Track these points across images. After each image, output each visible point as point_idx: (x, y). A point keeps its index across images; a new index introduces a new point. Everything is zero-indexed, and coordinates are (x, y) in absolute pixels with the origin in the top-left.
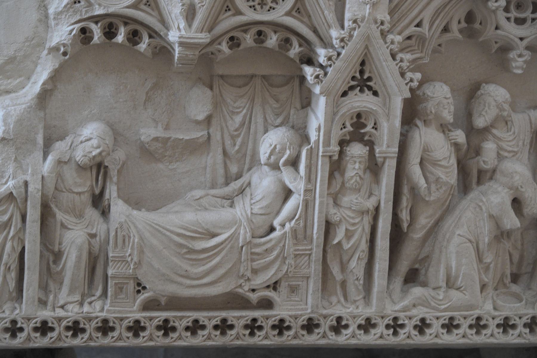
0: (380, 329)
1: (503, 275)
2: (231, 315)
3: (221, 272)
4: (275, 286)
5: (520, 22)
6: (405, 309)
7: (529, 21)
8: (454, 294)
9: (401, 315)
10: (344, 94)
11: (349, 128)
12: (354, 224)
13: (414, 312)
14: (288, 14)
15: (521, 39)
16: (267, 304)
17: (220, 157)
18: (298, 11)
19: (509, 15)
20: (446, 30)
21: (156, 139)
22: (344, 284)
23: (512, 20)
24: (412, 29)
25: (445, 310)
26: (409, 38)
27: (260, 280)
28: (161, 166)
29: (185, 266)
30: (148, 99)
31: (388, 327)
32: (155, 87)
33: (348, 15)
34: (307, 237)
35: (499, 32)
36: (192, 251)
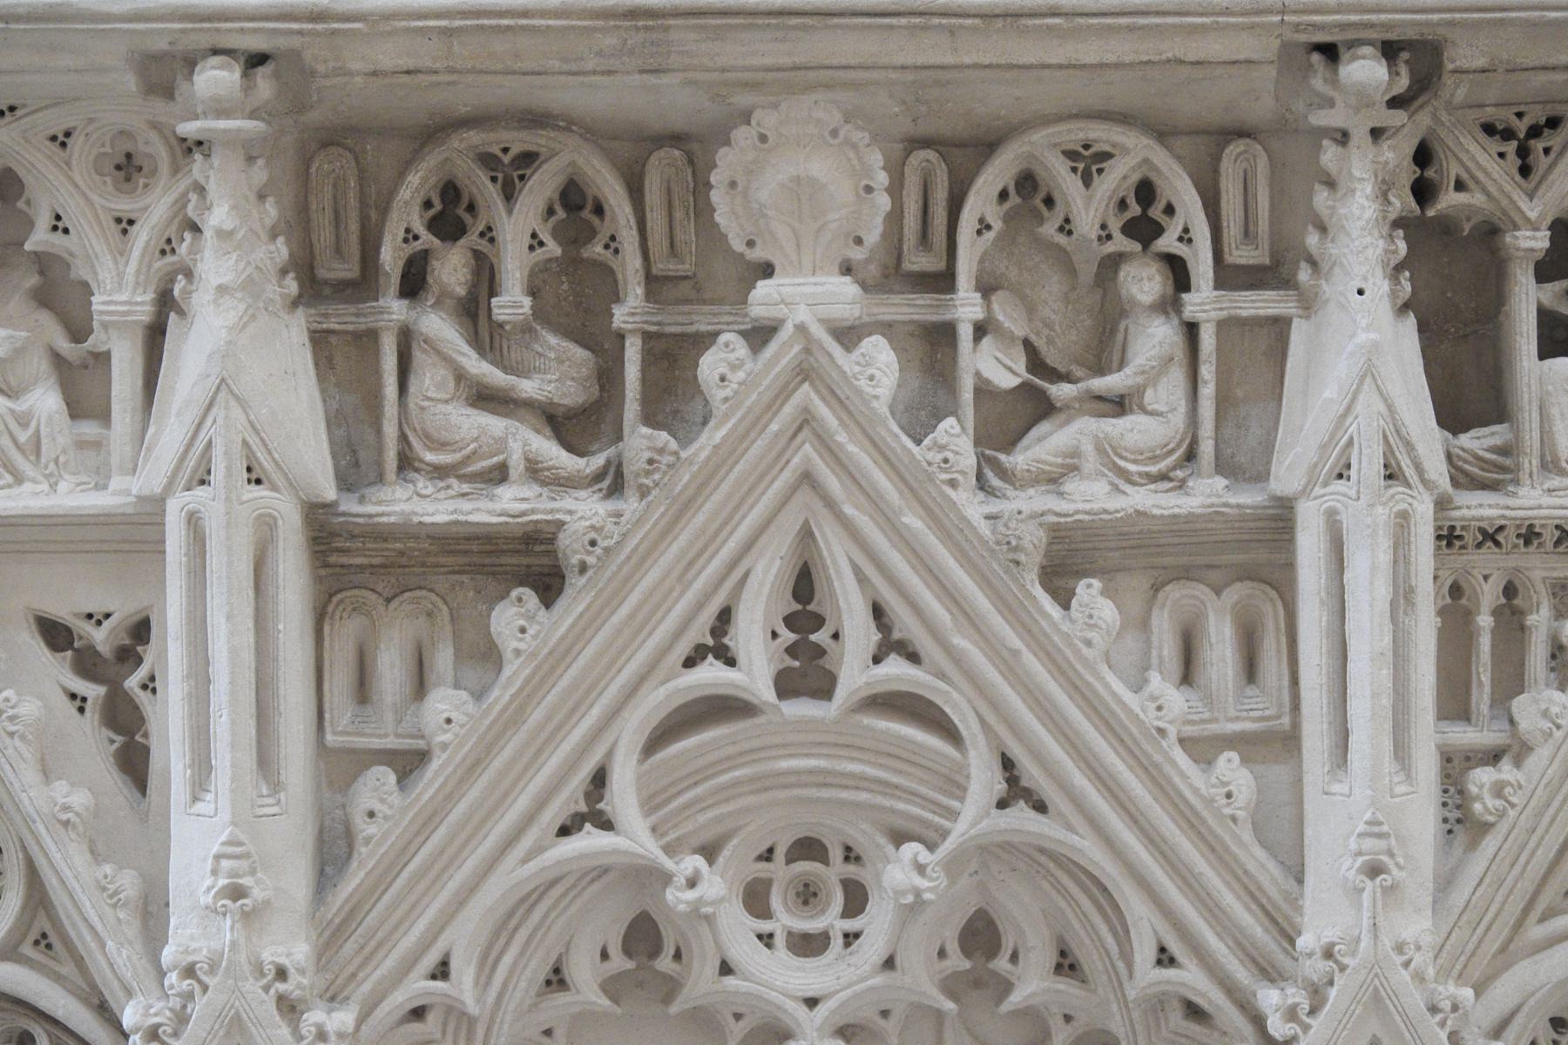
7: (837, 942)
15: (812, 1002)
18: (43, 941)
19: (765, 926)
20: (557, 980)
23: (780, 940)
24: (418, 987)
26: (418, 1013)
33: (168, 955)
35: (730, 981)
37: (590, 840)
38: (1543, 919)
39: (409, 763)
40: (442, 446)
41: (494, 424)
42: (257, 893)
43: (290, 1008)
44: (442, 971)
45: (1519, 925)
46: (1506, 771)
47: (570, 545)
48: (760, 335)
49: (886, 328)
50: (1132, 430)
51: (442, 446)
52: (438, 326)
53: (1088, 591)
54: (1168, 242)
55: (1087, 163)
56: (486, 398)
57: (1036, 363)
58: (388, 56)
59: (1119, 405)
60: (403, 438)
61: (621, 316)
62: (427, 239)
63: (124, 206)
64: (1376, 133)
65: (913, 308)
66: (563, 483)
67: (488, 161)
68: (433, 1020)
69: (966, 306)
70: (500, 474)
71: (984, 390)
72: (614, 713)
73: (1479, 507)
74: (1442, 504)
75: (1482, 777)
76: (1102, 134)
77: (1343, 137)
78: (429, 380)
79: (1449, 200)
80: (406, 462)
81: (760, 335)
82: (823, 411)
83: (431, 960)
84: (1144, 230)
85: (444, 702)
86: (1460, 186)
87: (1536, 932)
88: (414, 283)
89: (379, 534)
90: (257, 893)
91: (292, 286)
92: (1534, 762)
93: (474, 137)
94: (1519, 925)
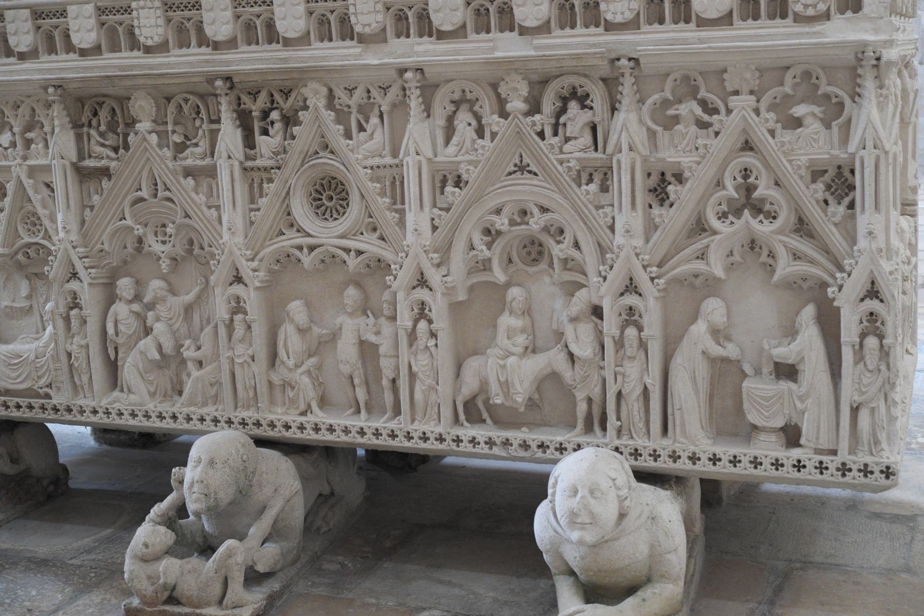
0: (100, 415)
1: (166, 390)
2: (32, 401)
3: (23, 376)
4: (49, 386)
5: (164, 243)
6: (110, 403)
8: (132, 396)
9: (108, 406)
10: (68, 281)
11: (69, 300)
12: (78, 353)
13: (115, 405)
14: (44, 238)
16: (48, 396)
17: (38, 318)
21: (6, 307)
22: (82, 388)
24: (99, 246)
25: (128, 405)
26: (102, 251)
27: (42, 382)
28: (14, 322)
29: (8, 372)
30: (5, 286)
31: (105, 413)
32: (7, 279)
34: (59, 360)
36: (10, 365)
37: (124, 222)
38: (270, 240)
39: (92, 208)
40: (95, 153)
41: (102, 149)
42: (68, 228)
43: (74, 247)
44: (103, 244)
45: (264, 241)
46: (256, 213)
47: (112, 171)
48: (136, 134)
49: (156, 132)
50: (198, 150)
51: (95, 153)
52: (93, 132)
53: (190, 179)
54: (200, 115)
55: (186, 100)
56: (103, 145)
57: (186, 137)
58: (75, 85)
59: (196, 145)
60: (89, 152)
61: (119, 130)
62: (91, 117)
63: (47, 112)
64: (227, 94)
65: (161, 128)
66: (113, 159)
67: (98, 103)
68: (103, 253)
69: (170, 127)
70: (102, 158)
71: (176, 144)
72: (123, 199)
73: (249, 164)
74: (241, 163)
75: (252, 213)
76: (191, 97)
77: (221, 96)
78: (93, 142)
79: (242, 106)
80: (90, 156)
81: (136, 134)
82: (148, 147)
83: (100, 241)
84: (198, 113)
85: (96, 199)
86: (244, 104)
87: (268, 243)
88: (90, 125)
89: (86, 168)
90: (68, 228)
91: (71, 125)
92: (261, 211)
93: (94, 99)
94: (264, 241)
